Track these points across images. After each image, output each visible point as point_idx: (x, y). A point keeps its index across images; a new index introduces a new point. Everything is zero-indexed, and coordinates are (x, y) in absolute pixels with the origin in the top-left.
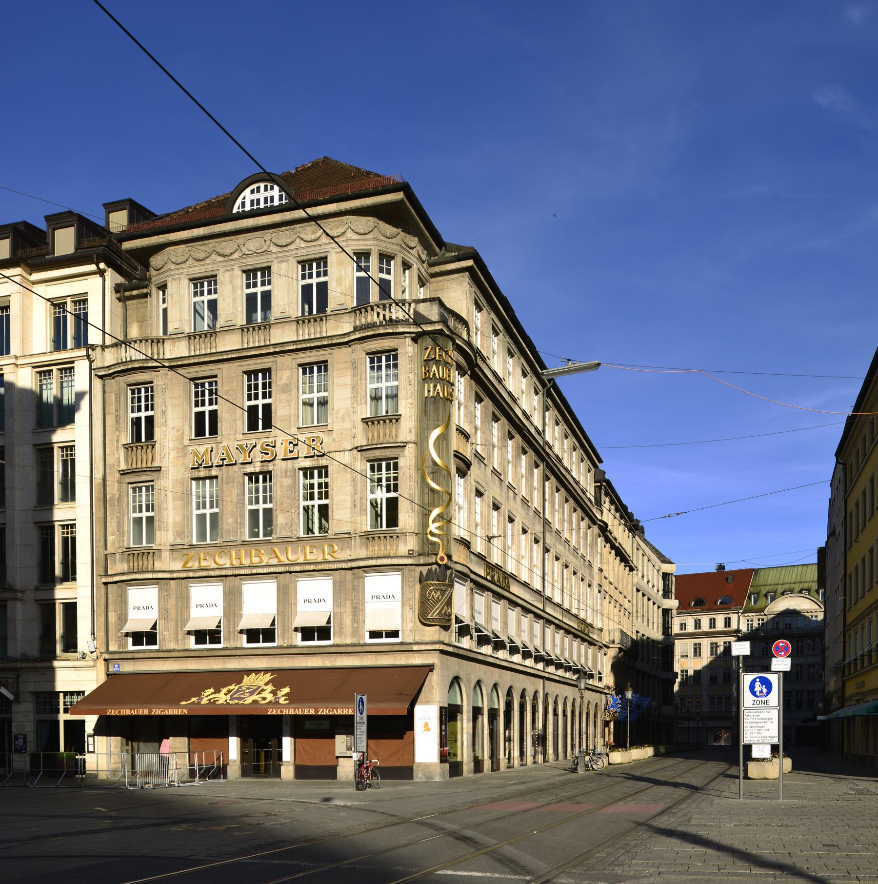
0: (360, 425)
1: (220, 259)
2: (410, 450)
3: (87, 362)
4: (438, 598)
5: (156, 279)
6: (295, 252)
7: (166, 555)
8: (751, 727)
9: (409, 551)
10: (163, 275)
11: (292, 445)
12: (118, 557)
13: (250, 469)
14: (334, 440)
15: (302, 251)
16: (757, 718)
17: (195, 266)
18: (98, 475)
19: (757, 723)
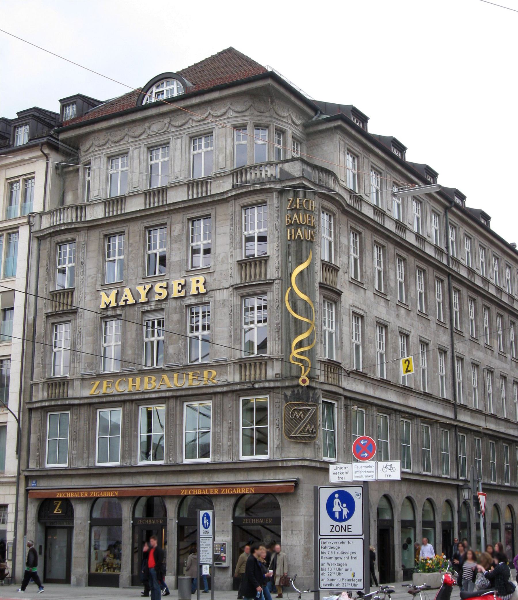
0: (236, 267)
1: (131, 140)
2: (276, 286)
3: (28, 227)
4: (300, 417)
5: (83, 159)
6: (188, 130)
7: (77, 383)
8: (329, 564)
9: (276, 374)
10: (89, 156)
11: (180, 286)
12: (41, 386)
13: (146, 308)
14: (215, 280)
15: (193, 129)
16: (336, 551)
17: (112, 147)
18: (31, 318)
19: (336, 558)
